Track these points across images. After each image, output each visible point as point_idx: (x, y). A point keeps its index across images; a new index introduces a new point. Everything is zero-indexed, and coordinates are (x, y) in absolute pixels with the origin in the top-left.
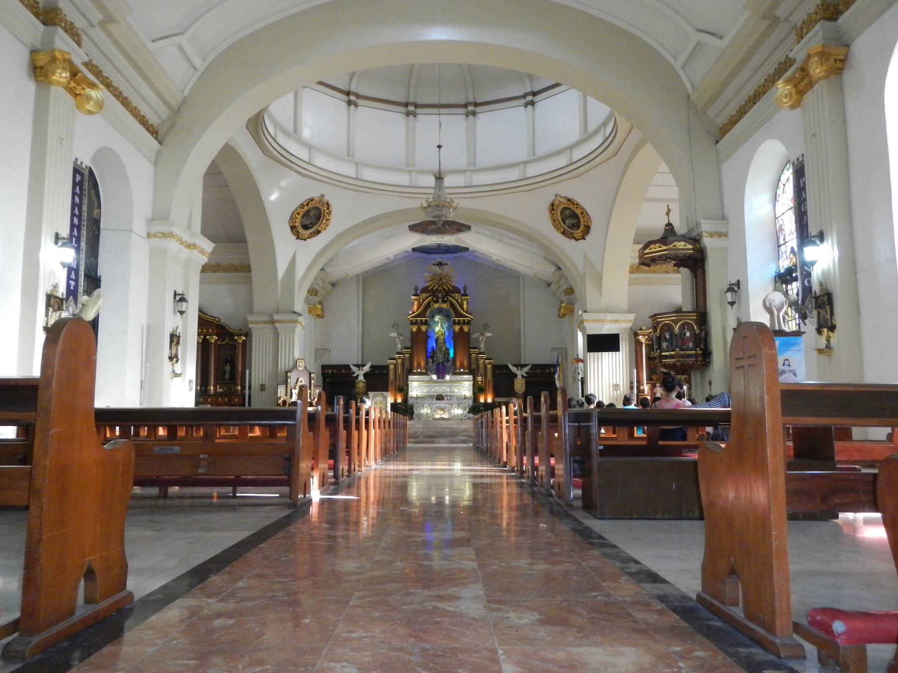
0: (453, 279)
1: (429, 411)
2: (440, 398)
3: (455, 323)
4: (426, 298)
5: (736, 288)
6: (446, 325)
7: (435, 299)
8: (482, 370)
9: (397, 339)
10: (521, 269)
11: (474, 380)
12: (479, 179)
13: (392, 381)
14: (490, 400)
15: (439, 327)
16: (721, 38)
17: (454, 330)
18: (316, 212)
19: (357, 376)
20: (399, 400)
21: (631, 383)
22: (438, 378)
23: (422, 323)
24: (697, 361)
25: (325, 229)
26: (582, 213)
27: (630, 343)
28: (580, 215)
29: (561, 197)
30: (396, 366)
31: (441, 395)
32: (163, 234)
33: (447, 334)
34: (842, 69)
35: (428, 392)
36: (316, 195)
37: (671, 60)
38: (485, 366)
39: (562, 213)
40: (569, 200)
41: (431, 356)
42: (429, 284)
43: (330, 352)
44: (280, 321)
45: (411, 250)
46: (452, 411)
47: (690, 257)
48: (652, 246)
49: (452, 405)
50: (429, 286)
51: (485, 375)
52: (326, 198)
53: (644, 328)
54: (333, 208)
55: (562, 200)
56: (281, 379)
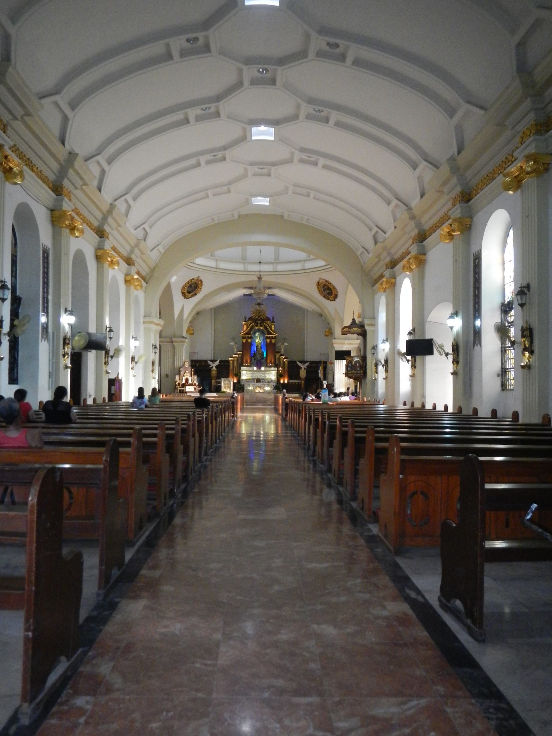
0: (266, 313)
1: (253, 388)
2: (258, 381)
3: (267, 338)
4: (251, 324)
5: (376, 348)
6: (262, 338)
7: (256, 324)
8: (282, 365)
9: (234, 346)
11: (278, 370)
12: (280, 267)
14: (286, 382)
15: (258, 340)
17: (267, 343)
18: (195, 285)
19: (212, 367)
20: (235, 381)
22: (257, 369)
23: (249, 338)
24: (361, 375)
25: (199, 293)
26: (333, 288)
29: (322, 279)
30: (233, 361)
31: (259, 379)
32: (150, 322)
33: (262, 343)
34: (395, 285)
35: (251, 376)
36: (195, 277)
38: (284, 362)
39: (323, 287)
40: (327, 281)
41: (253, 356)
42: (252, 315)
43: (198, 354)
44: (176, 342)
45: (242, 295)
46: (265, 388)
48: (345, 329)
49: (264, 385)
50: (252, 317)
51: (283, 368)
52: (201, 278)
54: (204, 283)
55: (323, 281)
56: (177, 371)
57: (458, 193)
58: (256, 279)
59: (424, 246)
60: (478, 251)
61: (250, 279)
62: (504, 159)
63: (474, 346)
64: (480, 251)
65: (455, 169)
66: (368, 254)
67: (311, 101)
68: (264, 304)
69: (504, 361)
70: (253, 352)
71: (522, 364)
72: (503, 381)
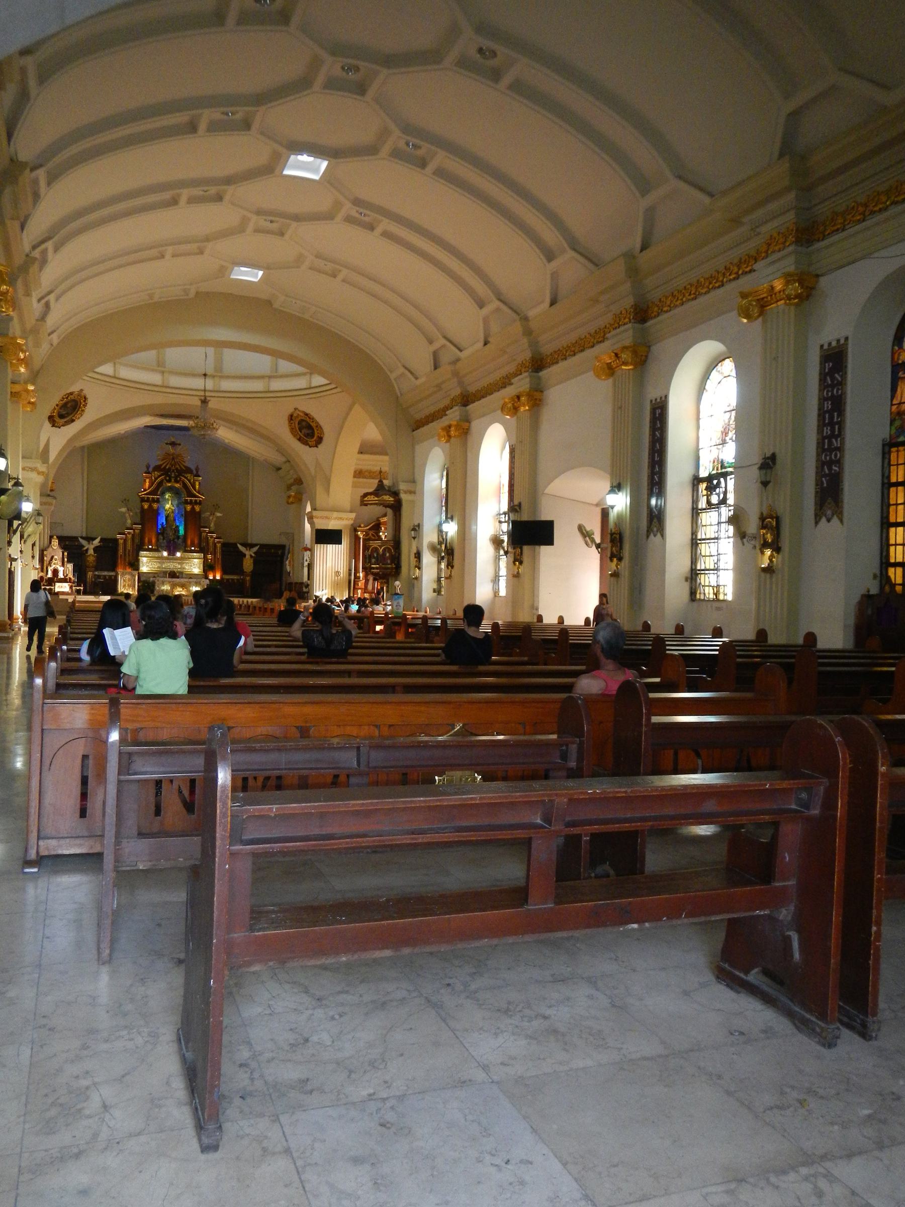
3: (186, 502)
6: (176, 502)
9: (127, 515)
10: (252, 453)
11: (205, 557)
13: (121, 556)
14: (218, 577)
16: (416, 378)
17: (185, 509)
19: (87, 550)
21: (350, 570)
23: (154, 501)
26: (317, 426)
27: (350, 536)
28: (315, 428)
30: (125, 540)
37: (389, 373)
38: (215, 545)
40: (307, 415)
42: (161, 463)
46: (191, 589)
47: (392, 504)
49: (190, 582)
50: (161, 465)
51: (214, 553)
52: (86, 392)
53: (362, 525)
54: (89, 401)
57: (628, 307)
58: (199, 403)
59: (539, 378)
60: (661, 398)
61: (181, 402)
62: (722, 269)
63: (648, 537)
64: (666, 397)
65: (633, 272)
66: (413, 379)
67: (408, 129)
68: (182, 444)
69: (694, 560)
70: (160, 527)
71: (763, 566)
72: (694, 587)
